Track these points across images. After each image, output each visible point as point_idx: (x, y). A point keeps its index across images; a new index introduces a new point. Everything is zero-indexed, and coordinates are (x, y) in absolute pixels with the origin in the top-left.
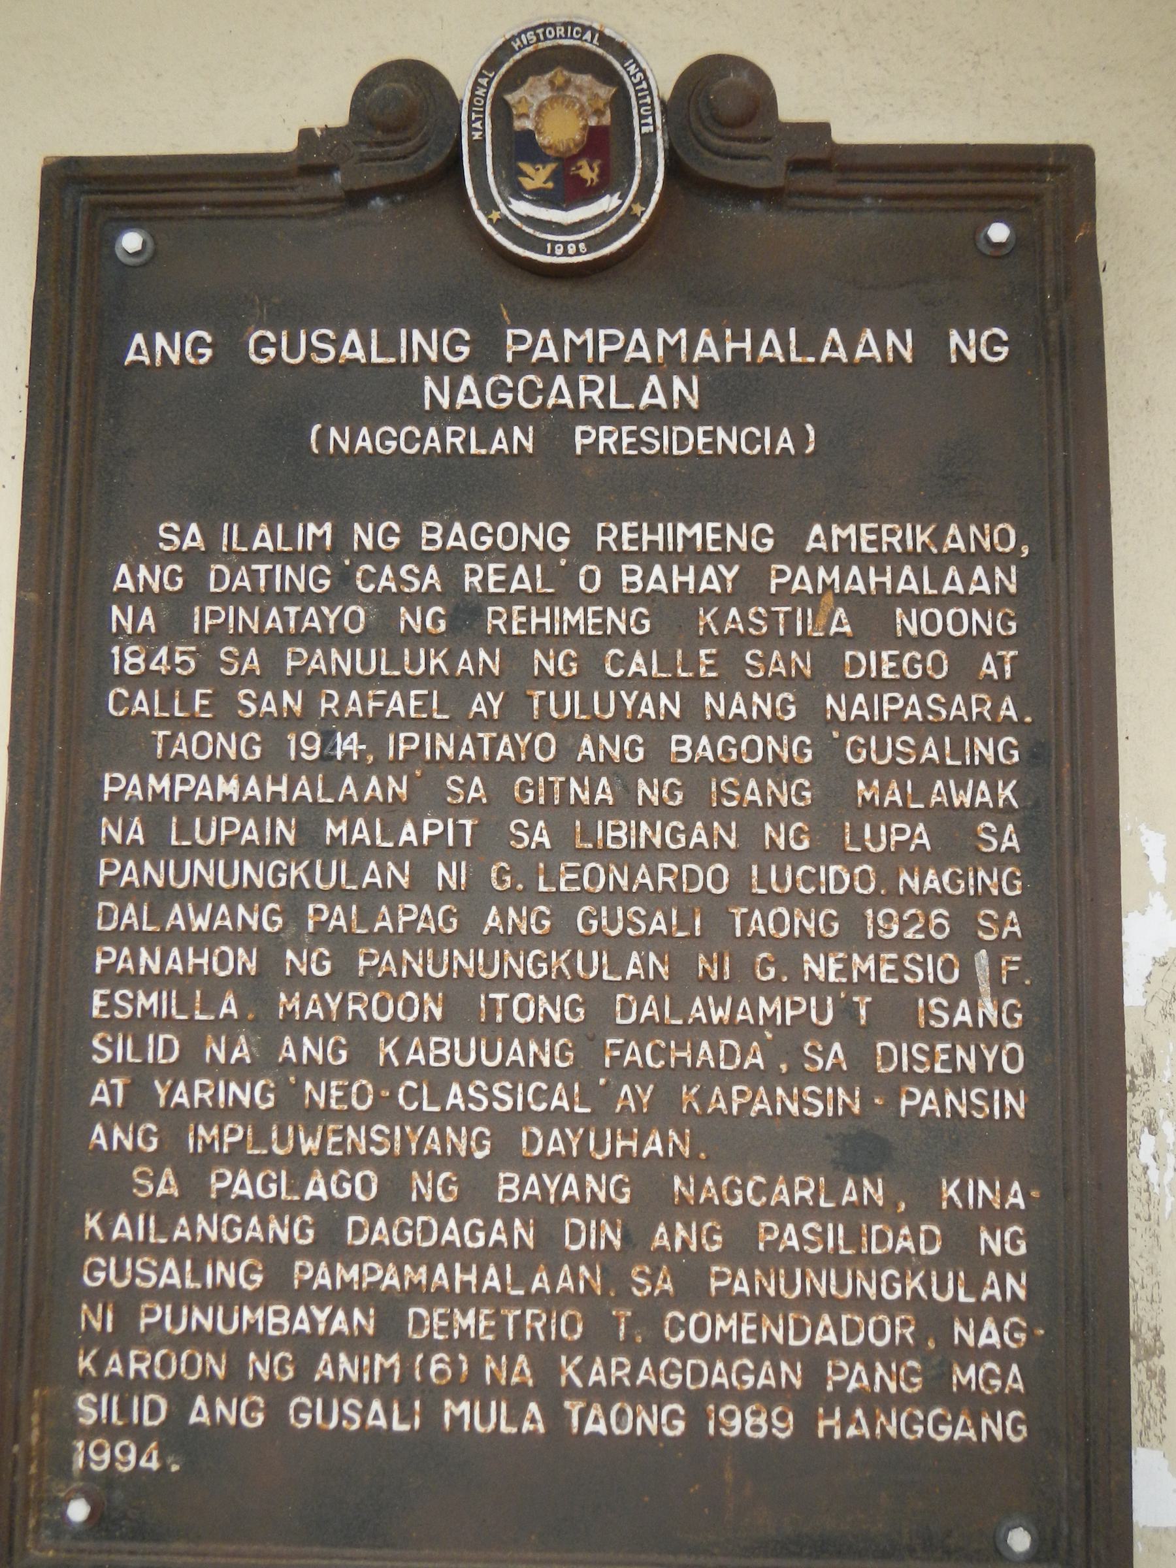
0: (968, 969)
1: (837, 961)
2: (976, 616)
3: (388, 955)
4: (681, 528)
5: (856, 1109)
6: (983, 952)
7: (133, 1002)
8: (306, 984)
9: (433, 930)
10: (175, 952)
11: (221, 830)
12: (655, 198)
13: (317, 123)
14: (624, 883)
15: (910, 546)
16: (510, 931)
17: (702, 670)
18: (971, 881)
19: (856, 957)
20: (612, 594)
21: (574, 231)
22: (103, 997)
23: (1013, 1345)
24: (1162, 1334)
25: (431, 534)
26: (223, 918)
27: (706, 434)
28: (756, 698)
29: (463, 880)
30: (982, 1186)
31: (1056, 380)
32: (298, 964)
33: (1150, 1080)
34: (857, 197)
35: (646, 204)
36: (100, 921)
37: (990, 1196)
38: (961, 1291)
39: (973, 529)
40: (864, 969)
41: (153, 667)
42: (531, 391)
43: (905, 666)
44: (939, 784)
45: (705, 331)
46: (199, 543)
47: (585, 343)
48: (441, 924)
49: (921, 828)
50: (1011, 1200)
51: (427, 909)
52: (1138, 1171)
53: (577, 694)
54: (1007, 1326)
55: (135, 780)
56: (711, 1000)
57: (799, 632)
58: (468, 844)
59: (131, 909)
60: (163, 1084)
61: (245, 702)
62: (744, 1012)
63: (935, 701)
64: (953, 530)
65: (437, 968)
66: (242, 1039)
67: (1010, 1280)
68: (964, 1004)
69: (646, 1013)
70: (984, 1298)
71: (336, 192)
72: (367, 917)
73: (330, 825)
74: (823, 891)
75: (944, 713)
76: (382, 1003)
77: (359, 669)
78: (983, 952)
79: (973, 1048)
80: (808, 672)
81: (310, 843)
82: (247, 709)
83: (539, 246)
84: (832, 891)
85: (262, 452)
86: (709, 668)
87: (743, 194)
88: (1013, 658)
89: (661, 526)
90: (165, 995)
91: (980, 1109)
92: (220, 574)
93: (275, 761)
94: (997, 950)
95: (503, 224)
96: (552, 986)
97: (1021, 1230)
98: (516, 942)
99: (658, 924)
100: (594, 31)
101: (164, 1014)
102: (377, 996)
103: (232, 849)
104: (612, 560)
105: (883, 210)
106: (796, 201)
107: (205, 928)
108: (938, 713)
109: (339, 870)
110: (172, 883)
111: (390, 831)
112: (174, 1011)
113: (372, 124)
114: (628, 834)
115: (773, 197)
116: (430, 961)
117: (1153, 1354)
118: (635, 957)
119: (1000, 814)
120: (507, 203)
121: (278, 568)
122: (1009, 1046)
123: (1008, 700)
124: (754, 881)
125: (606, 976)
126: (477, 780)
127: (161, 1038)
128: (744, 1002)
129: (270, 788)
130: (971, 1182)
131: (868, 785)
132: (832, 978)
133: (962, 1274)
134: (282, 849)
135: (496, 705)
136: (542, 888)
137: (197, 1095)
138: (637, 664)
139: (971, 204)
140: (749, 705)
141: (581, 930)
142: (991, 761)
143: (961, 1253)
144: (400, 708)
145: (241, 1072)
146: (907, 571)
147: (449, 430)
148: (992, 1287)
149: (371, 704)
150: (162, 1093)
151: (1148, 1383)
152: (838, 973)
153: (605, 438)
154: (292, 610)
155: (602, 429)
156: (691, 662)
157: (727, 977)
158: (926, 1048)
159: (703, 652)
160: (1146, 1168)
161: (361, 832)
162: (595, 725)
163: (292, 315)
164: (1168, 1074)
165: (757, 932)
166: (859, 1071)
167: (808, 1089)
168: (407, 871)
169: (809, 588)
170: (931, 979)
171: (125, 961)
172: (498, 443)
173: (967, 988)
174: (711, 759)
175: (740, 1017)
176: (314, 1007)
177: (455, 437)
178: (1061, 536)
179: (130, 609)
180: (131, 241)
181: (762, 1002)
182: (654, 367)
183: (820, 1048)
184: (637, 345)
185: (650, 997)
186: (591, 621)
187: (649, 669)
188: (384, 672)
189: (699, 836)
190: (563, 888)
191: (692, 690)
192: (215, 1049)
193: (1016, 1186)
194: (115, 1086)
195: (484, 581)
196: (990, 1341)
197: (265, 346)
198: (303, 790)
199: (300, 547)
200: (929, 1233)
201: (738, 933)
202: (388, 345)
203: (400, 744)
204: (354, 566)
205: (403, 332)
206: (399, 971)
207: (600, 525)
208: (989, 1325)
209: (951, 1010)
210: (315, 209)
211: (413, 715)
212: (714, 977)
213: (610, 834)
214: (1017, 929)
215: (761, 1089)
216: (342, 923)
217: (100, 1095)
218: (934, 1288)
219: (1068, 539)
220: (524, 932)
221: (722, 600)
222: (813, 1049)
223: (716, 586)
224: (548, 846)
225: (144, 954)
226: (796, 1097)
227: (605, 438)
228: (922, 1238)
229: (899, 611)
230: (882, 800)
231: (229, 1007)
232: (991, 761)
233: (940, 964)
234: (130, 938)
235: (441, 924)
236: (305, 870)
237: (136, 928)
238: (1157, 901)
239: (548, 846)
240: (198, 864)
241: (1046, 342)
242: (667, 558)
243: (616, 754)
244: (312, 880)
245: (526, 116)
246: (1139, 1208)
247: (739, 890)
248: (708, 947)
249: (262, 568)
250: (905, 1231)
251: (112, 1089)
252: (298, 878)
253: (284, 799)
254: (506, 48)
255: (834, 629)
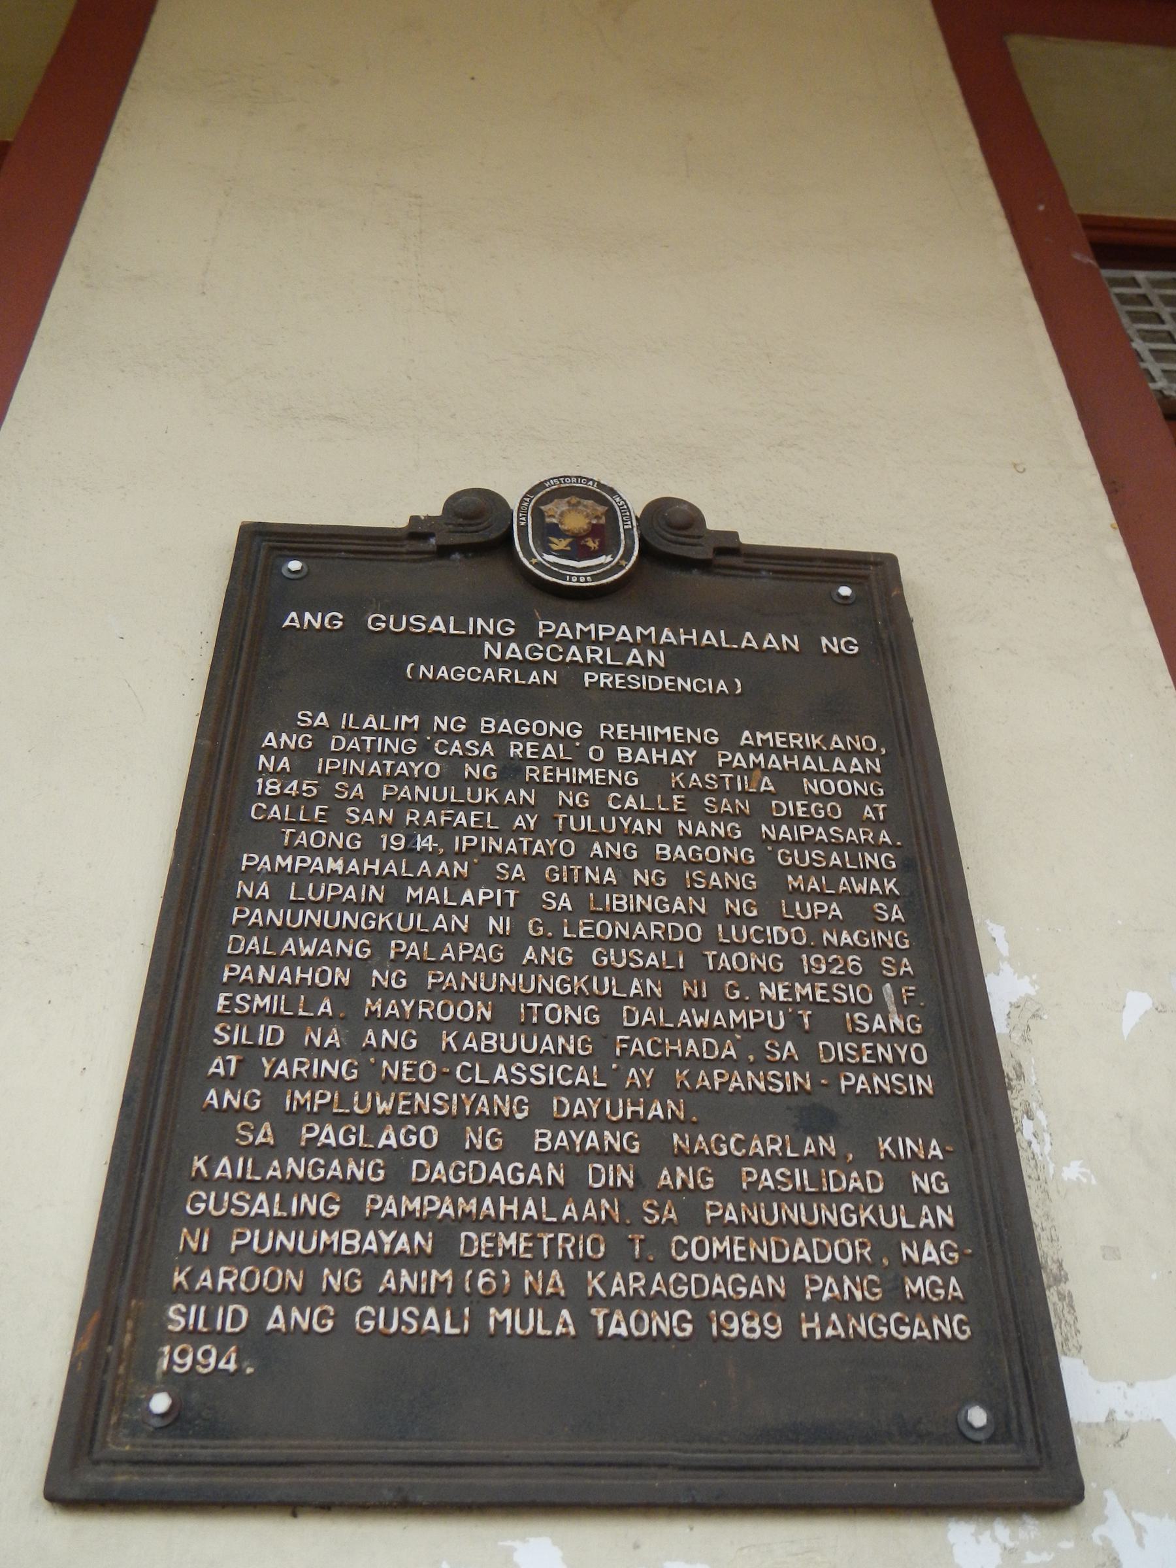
0: (878, 995)
1: (784, 987)
2: (856, 784)
3: (451, 975)
4: (657, 729)
5: (808, 1086)
6: (888, 985)
7: (251, 1002)
8: (387, 993)
9: (485, 960)
10: (287, 970)
11: (327, 891)
12: (634, 558)
13: (422, 514)
14: (626, 933)
15: (808, 745)
16: (543, 962)
17: (675, 807)
18: (874, 938)
19: (797, 985)
20: (611, 761)
21: (581, 573)
22: (226, 999)
23: (949, 1262)
24: (1064, 1266)
25: (488, 724)
26: (326, 948)
27: (670, 680)
28: (713, 824)
29: (508, 928)
30: (909, 1142)
31: (890, 661)
32: (381, 979)
33: (1022, 1082)
34: (757, 570)
35: (628, 560)
36: (230, 947)
37: (916, 1149)
38: (903, 1220)
39: (848, 738)
40: (804, 993)
41: (286, 791)
42: (554, 652)
43: (813, 810)
44: (844, 879)
45: (666, 629)
46: (325, 723)
47: (590, 631)
48: (491, 956)
49: (834, 905)
50: (932, 1153)
51: (480, 946)
52: (1025, 1145)
53: (589, 818)
54: (942, 1247)
55: (266, 858)
56: (693, 1011)
57: (740, 788)
58: (512, 905)
59: (255, 940)
60: (268, 1061)
61: (351, 815)
62: (719, 1020)
63: (835, 831)
64: (836, 738)
65: (487, 985)
66: (335, 1030)
67: (940, 1211)
68: (878, 1017)
69: (646, 1019)
70: (921, 1225)
71: (430, 548)
72: (435, 950)
73: (410, 890)
74: (770, 942)
75: (842, 838)
76: (445, 1008)
77: (434, 798)
78: (888, 985)
79: (889, 1047)
80: (748, 811)
81: (395, 902)
82: (353, 819)
83: (563, 577)
84: (776, 942)
85: (376, 677)
86: (680, 806)
87: (687, 564)
88: (884, 809)
89: (643, 728)
90: (276, 997)
91: (900, 1088)
92: (338, 742)
93: (370, 850)
94: (897, 981)
95: (538, 565)
96: (575, 999)
97: (942, 1175)
98: (547, 969)
99: (652, 960)
100: (594, 481)
101: (275, 1010)
102: (441, 1003)
103: (337, 903)
104: (611, 744)
105: (774, 579)
106: (718, 570)
107: (311, 953)
108: (838, 838)
109: (415, 920)
110: (289, 924)
111: (455, 895)
112: (282, 1009)
113: (458, 515)
114: (628, 903)
115: (704, 566)
116: (483, 980)
117: (1060, 1281)
118: (636, 982)
119: (890, 898)
120: (541, 556)
121: (380, 739)
122: (915, 1045)
123: (884, 832)
124: (720, 934)
125: (614, 993)
126: (518, 866)
127: (270, 1028)
128: (719, 1013)
129: (366, 866)
130: (900, 1139)
131: (795, 879)
132: (781, 998)
133: (902, 1207)
134: (373, 904)
135: (532, 822)
136: (566, 935)
137: (296, 1069)
138: (630, 802)
139: (827, 579)
140: (708, 829)
141: (596, 963)
142: (878, 866)
143: (899, 1190)
144: (464, 821)
145: (331, 1053)
146: (808, 758)
147: (500, 670)
148: (927, 1217)
149: (443, 818)
150: (268, 1066)
151: (1060, 1304)
152: (786, 995)
153: (604, 679)
154: (389, 763)
155: (602, 675)
156: (668, 802)
157: (704, 996)
158: (855, 1046)
159: (675, 797)
160: (1030, 1143)
161: (432, 895)
162: (602, 836)
163: (398, 607)
164: (1034, 1079)
165: (724, 968)
166: (806, 1060)
167: (771, 1073)
168: (466, 921)
169: (744, 765)
170: (853, 1000)
171: (247, 974)
172: (534, 678)
173: (879, 1006)
174: (684, 859)
175: (716, 1023)
176: (393, 1009)
177: (503, 674)
178: (905, 741)
179: (273, 758)
180: (295, 565)
181: (732, 1013)
182: (635, 644)
183: (777, 1045)
184: (623, 633)
185: (649, 1009)
186: (597, 777)
187: (639, 805)
188: (453, 800)
189: (679, 906)
190: (581, 935)
191: (670, 816)
192: (313, 1036)
193: (934, 1142)
194: (230, 1061)
195: (524, 752)
196: (930, 1259)
197: (377, 621)
198: (391, 867)
199: (396, 728)
200: (873, 1176)
201: (711, 968)
202: (461, 624)
203: (463, 843)
204: (433, 741)
205: (471, 620)
206: (459, 986)
207: (602, 725)
208: (929, 1246)
209: (870, 1021)
210: (416, 557)
211: (472, 825)
212: (695, 995)
213: (615, 902)
214: (909, 969)
215: (736, 1072)
216: (416, 953)
217: (217, 1067)
218: (882, 1218)
219: (910, 745)
220: (553, 963)
221: (687, 769)
222: (771, 1045)
223: (682, 761)
224: (570, 908)
225: (262, 970)
226: (762, 1077)
227: (604, 679)
228: (868, 1180)
229: (805, 780)
230: (806, 889)
231: (326, 1006)
232: (878, 866)
233: (858, 991)
234: (253, 959)
235: (491, 956)
236: (390, 919)
237: (258, 952)
238: (1005, 967)
239: (570, 908)
240: (309, 912)
241: (882, 645)
242: (648, 744)
243: (618, 853)
244: (394, 925)
245: (553, 516)
246: (1030, 1171)
247: (710, 939)
248: (687, 976)
249: (369, 739)
250: (854, 1175)
251: (227, 1063)
252: (384, 924)
253: (377, 873)
254: (541, 485)
255: (763, 788)
